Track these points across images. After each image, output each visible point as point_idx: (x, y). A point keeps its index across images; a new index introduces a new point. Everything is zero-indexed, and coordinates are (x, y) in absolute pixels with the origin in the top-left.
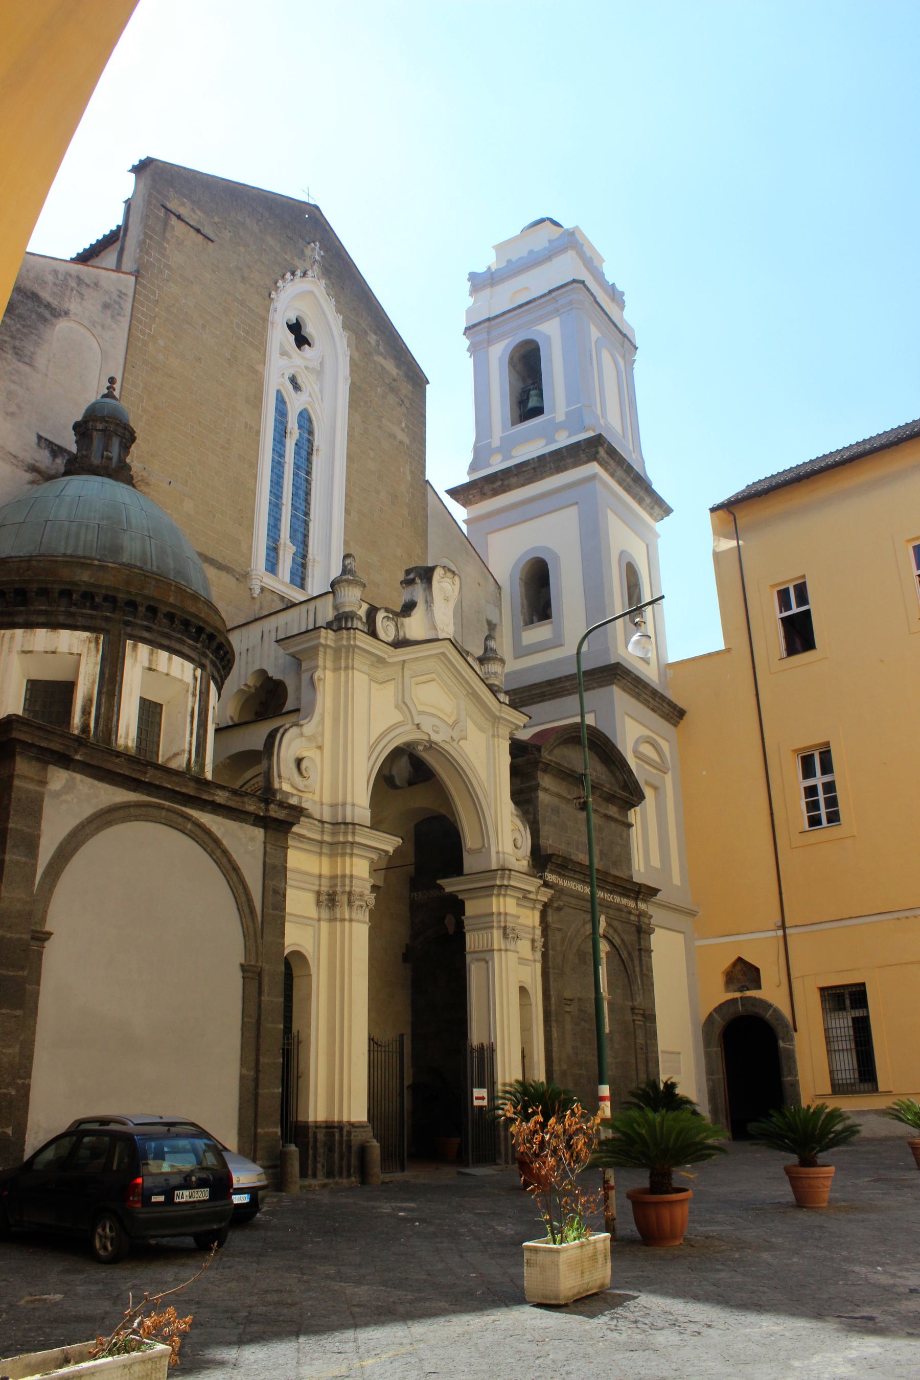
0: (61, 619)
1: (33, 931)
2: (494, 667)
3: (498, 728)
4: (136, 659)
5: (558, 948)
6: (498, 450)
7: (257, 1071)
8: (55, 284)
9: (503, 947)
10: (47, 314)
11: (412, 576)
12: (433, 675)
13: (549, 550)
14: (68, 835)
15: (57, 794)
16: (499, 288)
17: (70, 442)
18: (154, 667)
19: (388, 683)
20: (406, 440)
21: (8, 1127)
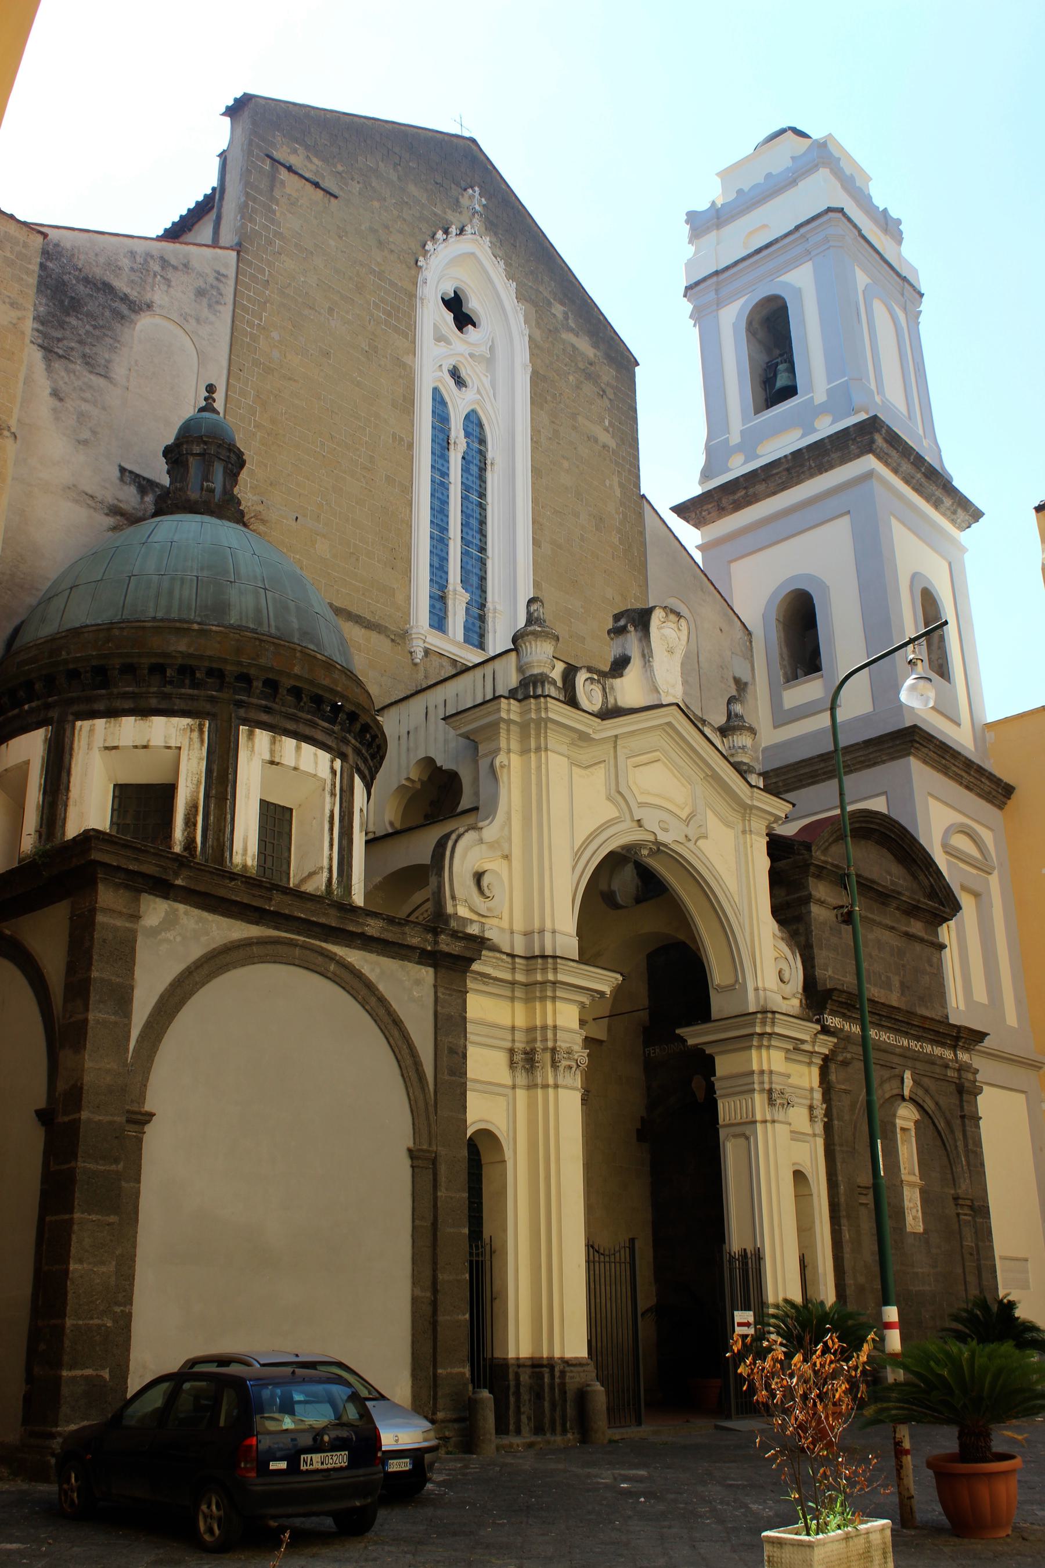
0: (153, 702)
1: (128, 1112)
2: (742, 740)
3: (749, 821)
4: (253, 751)
5: (847, 1117)
6: (739, 448)
7: (435, 1291)
8: (132, 269)
9: (768, 1118)
10: (124, 309)
11: (622, 623)
12: (658, 753)
13: (811, 578)
14: (171, 985)
15: (154, 932)
16: (728, 230)
17: (159, 472)
18: (277, 760)
19: (596, 767)
20: (612, 444)
21: (104, 1368)
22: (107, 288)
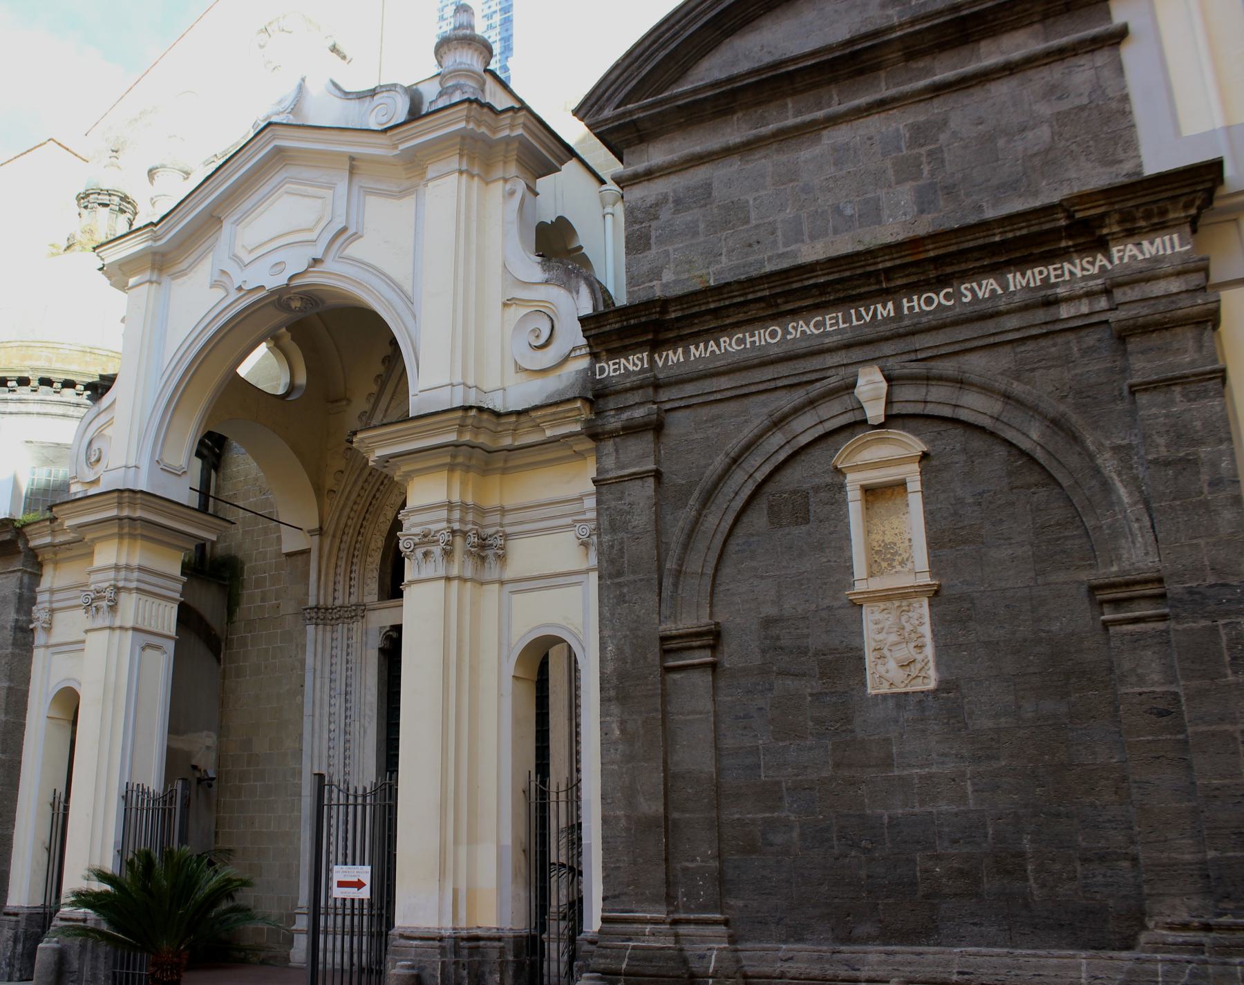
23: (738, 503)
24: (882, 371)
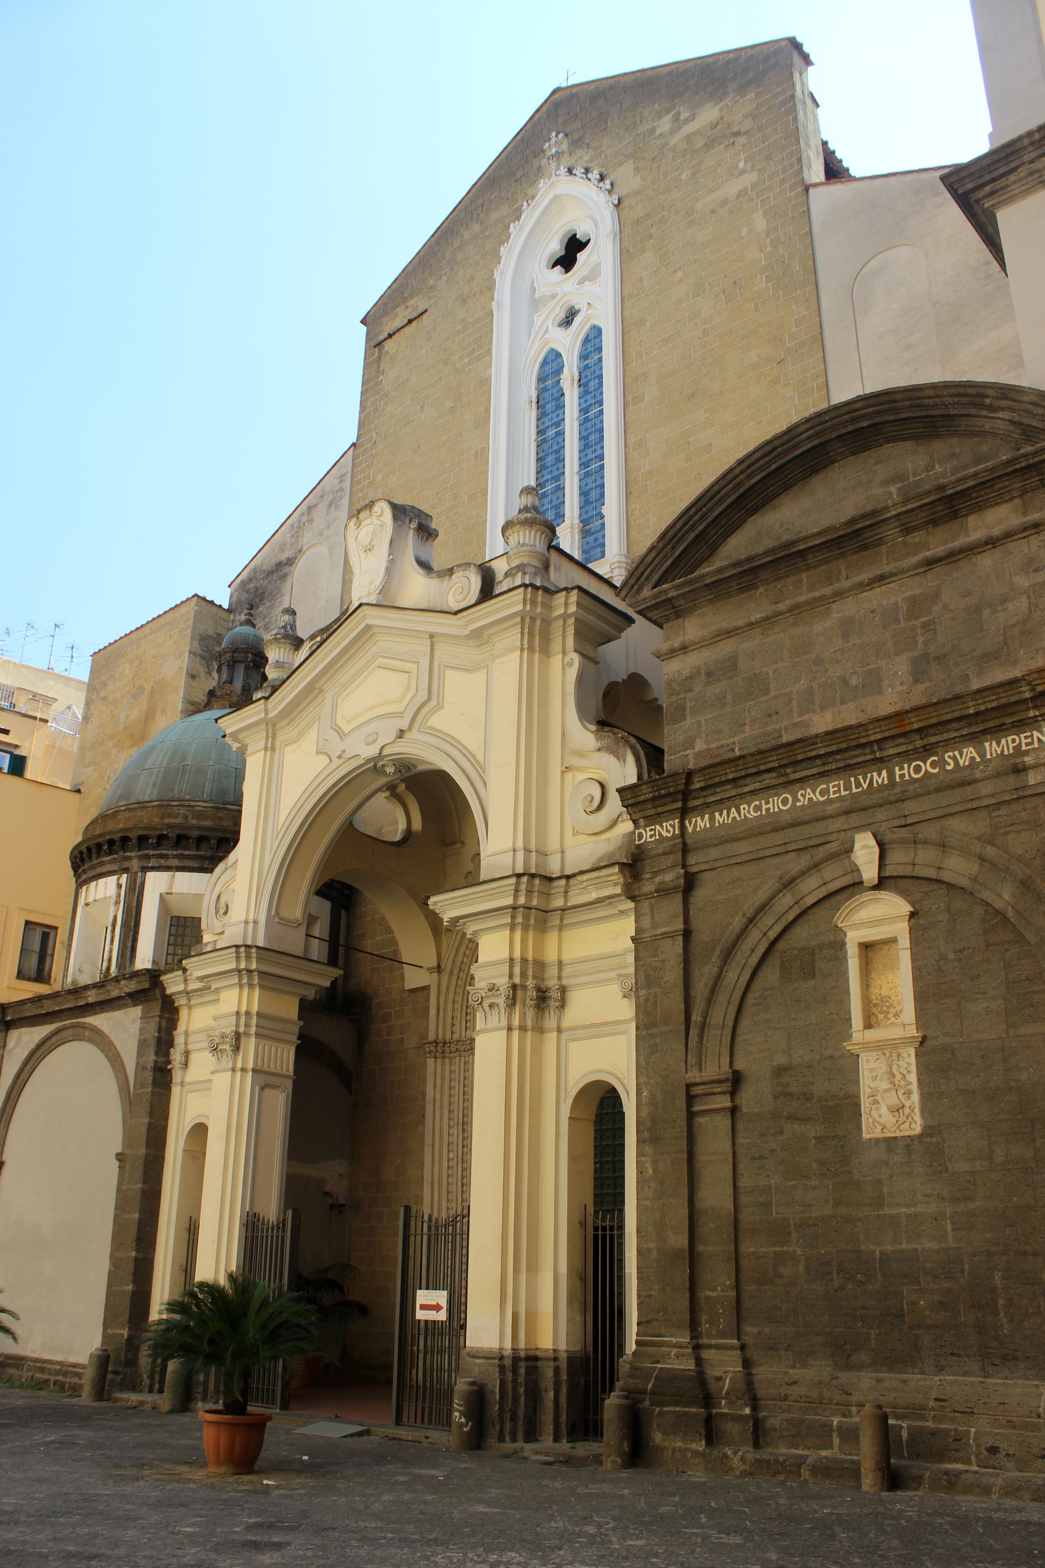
22: (279, 565)
23: (754, 960)
24: (875, 836)
